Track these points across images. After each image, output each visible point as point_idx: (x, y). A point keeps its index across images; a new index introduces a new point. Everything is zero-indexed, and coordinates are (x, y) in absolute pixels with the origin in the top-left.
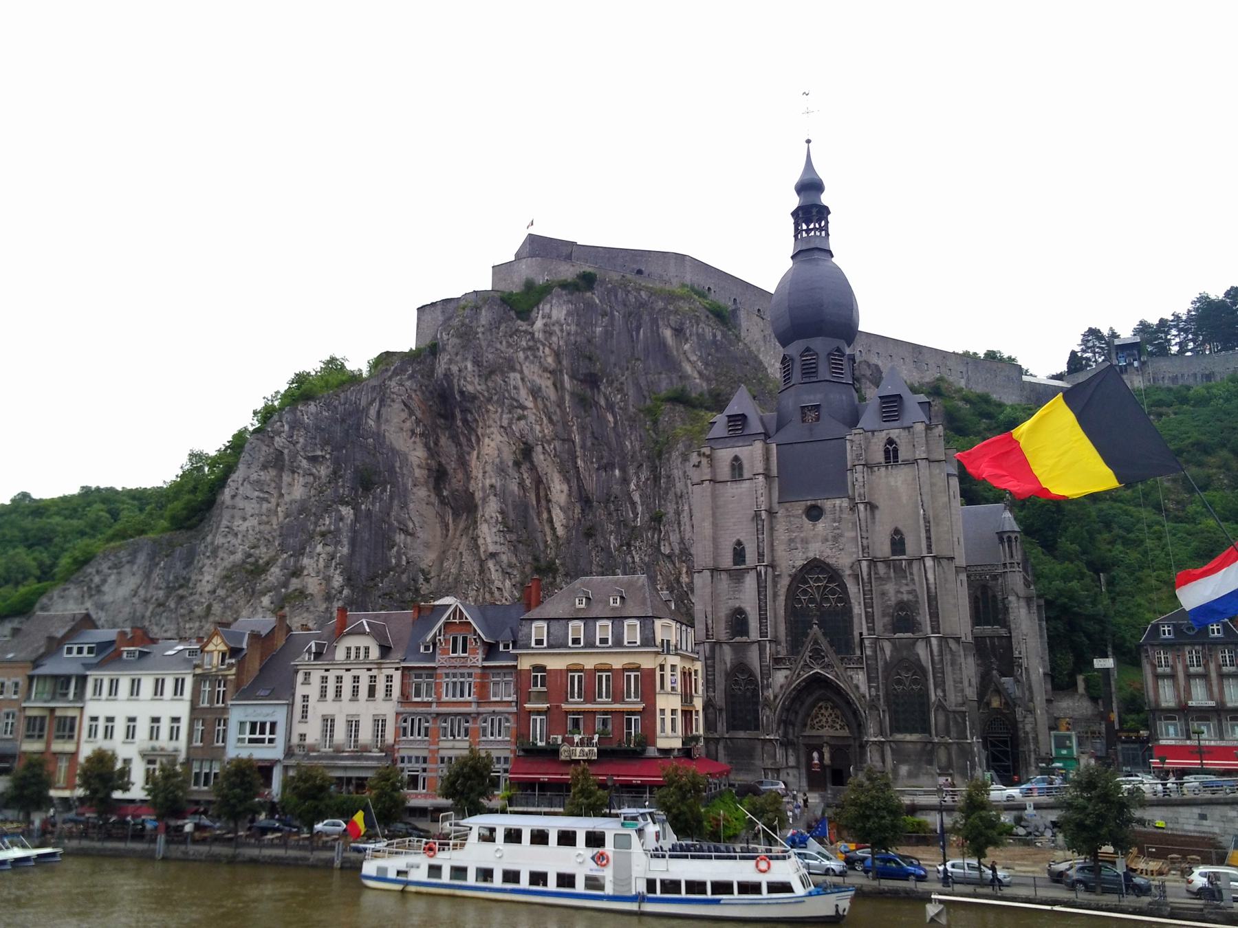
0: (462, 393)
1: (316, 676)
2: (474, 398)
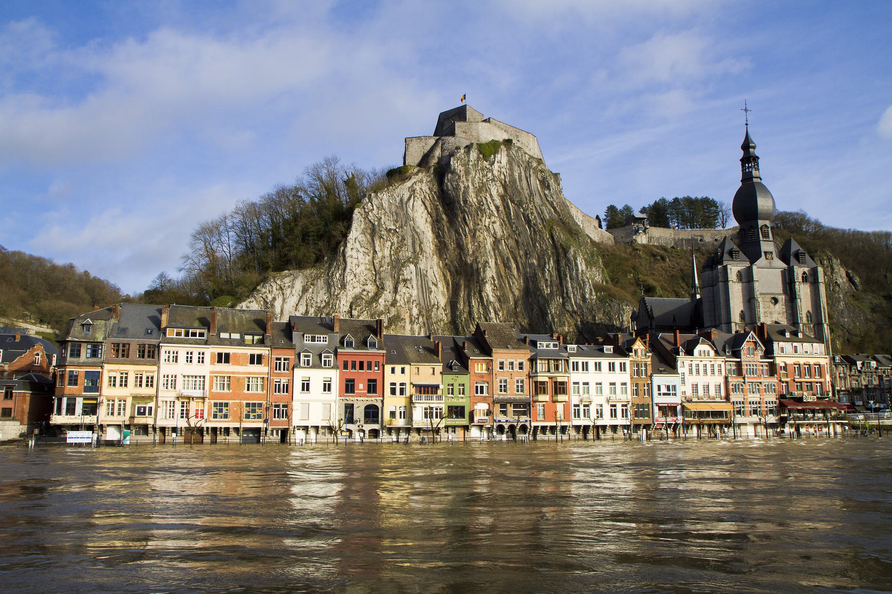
0: (465, 201)
1: (687, 363)
2: (472, 206)
